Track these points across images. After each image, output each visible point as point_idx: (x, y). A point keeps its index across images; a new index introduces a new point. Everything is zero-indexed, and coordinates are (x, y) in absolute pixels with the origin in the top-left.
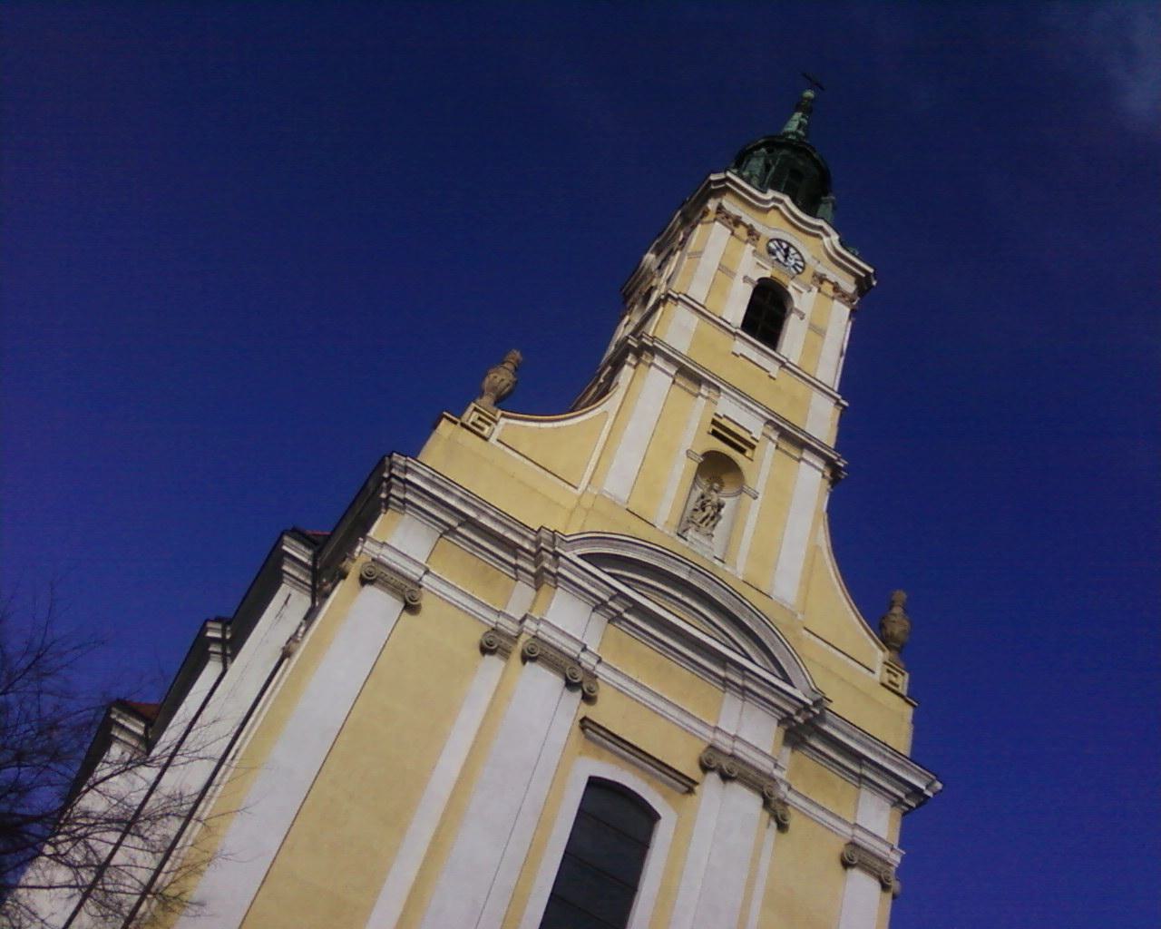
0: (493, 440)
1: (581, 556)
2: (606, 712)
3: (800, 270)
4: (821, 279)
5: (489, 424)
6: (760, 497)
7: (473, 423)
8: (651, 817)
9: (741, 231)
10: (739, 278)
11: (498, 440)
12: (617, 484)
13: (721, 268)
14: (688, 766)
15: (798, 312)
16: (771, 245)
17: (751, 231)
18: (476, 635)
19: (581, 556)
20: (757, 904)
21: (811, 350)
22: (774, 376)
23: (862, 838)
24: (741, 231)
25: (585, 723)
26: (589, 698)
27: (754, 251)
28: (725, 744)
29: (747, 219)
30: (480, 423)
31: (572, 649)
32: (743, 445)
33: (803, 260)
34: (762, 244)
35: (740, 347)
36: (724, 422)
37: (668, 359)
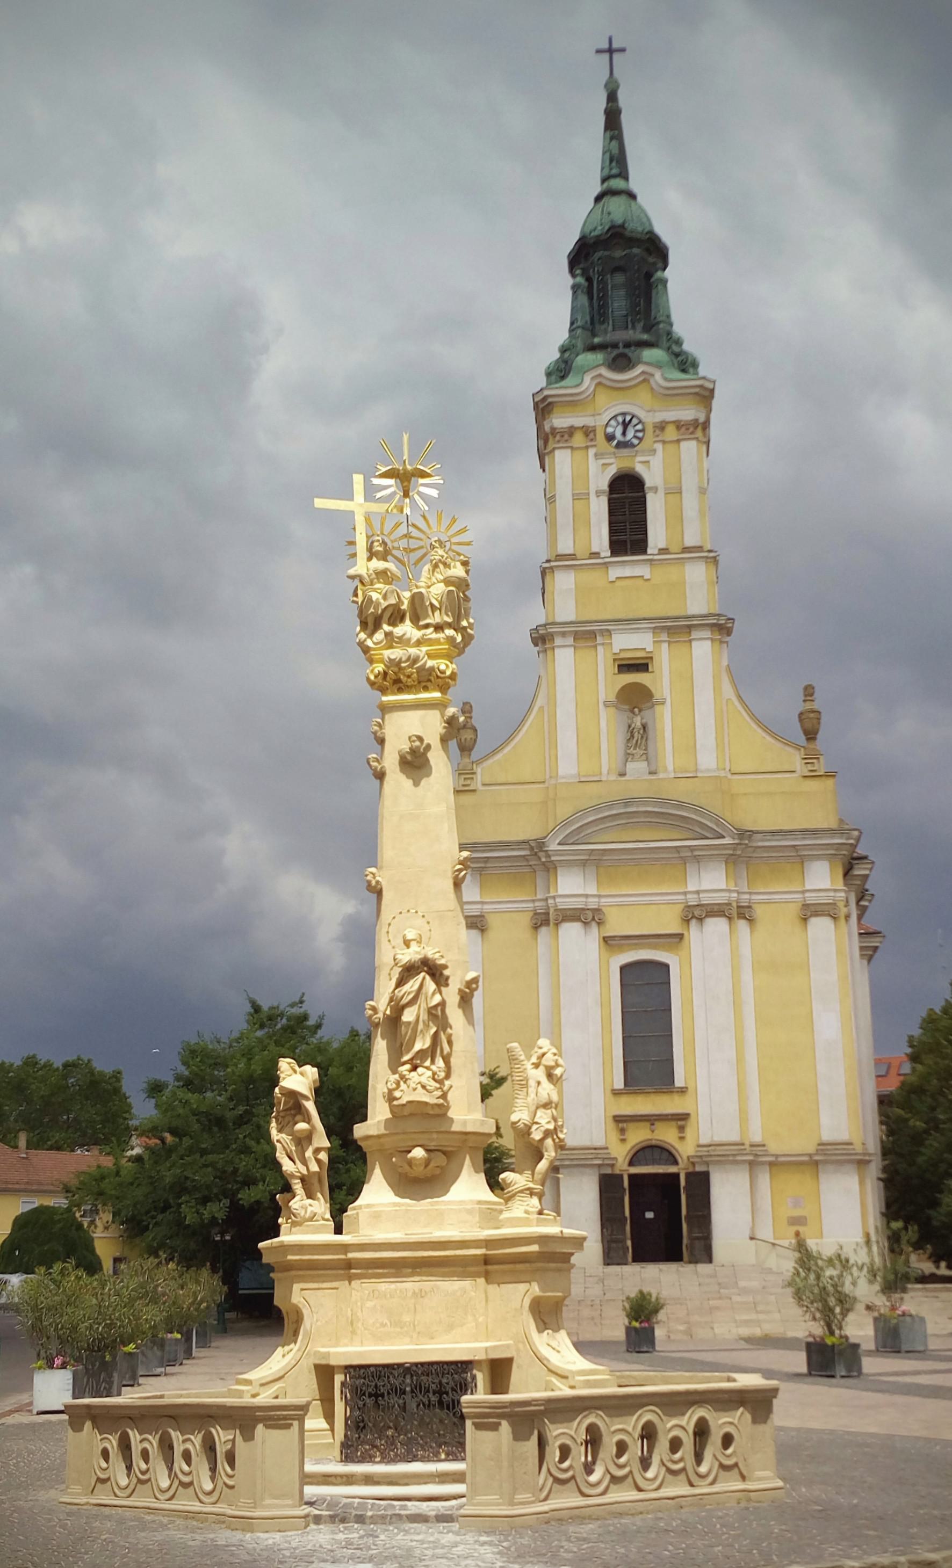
0: (480, 787)
1: (559, 844)
2: (618, 925)
3: (640, 435)
4: (661, 427)
5: (472, 778)
6: (669, 701)
7: (464, 785)
8: (666, 967)
9: (579, 439)
10: (593, 497)
11: (484, 785)
12: (567, 767)
13: (576, 497)
14: (674, 928)
15: (651, 488)
16: (610, 430)
17: (588, 432)
18: (525, 920)
19: (559, 844)
20: (747, 976)
21: (676, 518)
22: (648, 577)
23: (811, 898)
24: (579, 439)
25: (606, 940)
26: (600, 923)
27: (596, 455)
28: (693, 900)
29: (578, 421)
30: (468, 782)
31: (578, 903)
32: (641, 666)
33: (640, 422)
34: (600, 436)
35: (614, 573)
36: (623, 655)
37: (564, 634)
